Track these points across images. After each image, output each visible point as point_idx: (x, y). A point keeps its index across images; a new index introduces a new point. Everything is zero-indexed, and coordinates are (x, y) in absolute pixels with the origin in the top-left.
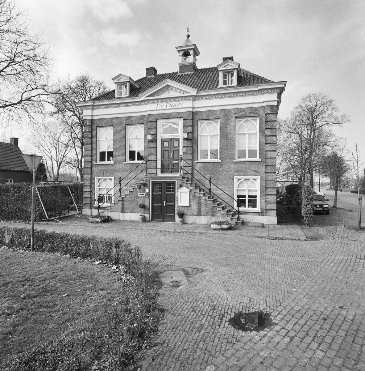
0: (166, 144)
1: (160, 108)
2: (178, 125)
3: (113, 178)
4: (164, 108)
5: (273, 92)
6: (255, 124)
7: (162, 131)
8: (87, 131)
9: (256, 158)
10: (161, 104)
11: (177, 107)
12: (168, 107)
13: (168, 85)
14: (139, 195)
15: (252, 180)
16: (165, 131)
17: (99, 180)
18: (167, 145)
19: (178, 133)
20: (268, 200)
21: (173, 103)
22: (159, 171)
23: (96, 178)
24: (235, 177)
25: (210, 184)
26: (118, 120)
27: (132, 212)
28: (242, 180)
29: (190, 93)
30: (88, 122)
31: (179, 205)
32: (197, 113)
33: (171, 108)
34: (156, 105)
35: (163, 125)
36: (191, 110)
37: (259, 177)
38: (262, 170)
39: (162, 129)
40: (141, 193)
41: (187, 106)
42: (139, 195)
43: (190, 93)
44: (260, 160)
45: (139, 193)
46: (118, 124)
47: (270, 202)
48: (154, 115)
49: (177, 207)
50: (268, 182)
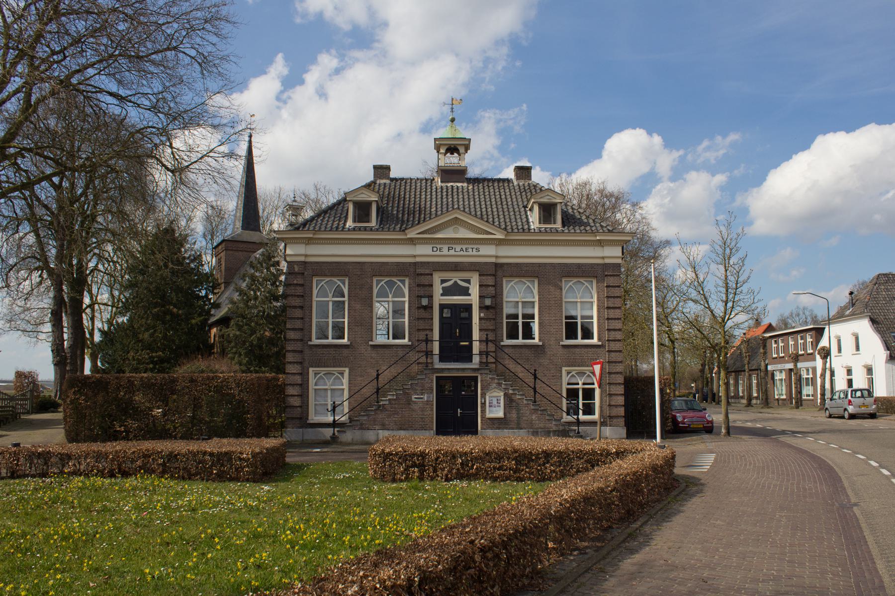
0: (447, 313)
2: (468, 281)
4: (445, 251)
5: (616, 245)
7: (441, 292)
8: (295, 282)
9: (593, 339)
11: (470, 253)
12: (452, 252)
15: (588, 373)
16: (446, 292)
18: (449, 315)
19: (469, 295)
20: (613, 403)
22: (436, 359)
23: (311, 369)
24: (564, 369)
25: (535, 380)
27: (401, 429)
28: (573, 373)
30: (296, 266)
32: (502, 265)
34: (430, 247)
35: (443, 281)
36: (493, 260)
39: (441, 287)
41: (488, 253)
46: (359, 273)
47: (616, 406)
50: (613, 376)
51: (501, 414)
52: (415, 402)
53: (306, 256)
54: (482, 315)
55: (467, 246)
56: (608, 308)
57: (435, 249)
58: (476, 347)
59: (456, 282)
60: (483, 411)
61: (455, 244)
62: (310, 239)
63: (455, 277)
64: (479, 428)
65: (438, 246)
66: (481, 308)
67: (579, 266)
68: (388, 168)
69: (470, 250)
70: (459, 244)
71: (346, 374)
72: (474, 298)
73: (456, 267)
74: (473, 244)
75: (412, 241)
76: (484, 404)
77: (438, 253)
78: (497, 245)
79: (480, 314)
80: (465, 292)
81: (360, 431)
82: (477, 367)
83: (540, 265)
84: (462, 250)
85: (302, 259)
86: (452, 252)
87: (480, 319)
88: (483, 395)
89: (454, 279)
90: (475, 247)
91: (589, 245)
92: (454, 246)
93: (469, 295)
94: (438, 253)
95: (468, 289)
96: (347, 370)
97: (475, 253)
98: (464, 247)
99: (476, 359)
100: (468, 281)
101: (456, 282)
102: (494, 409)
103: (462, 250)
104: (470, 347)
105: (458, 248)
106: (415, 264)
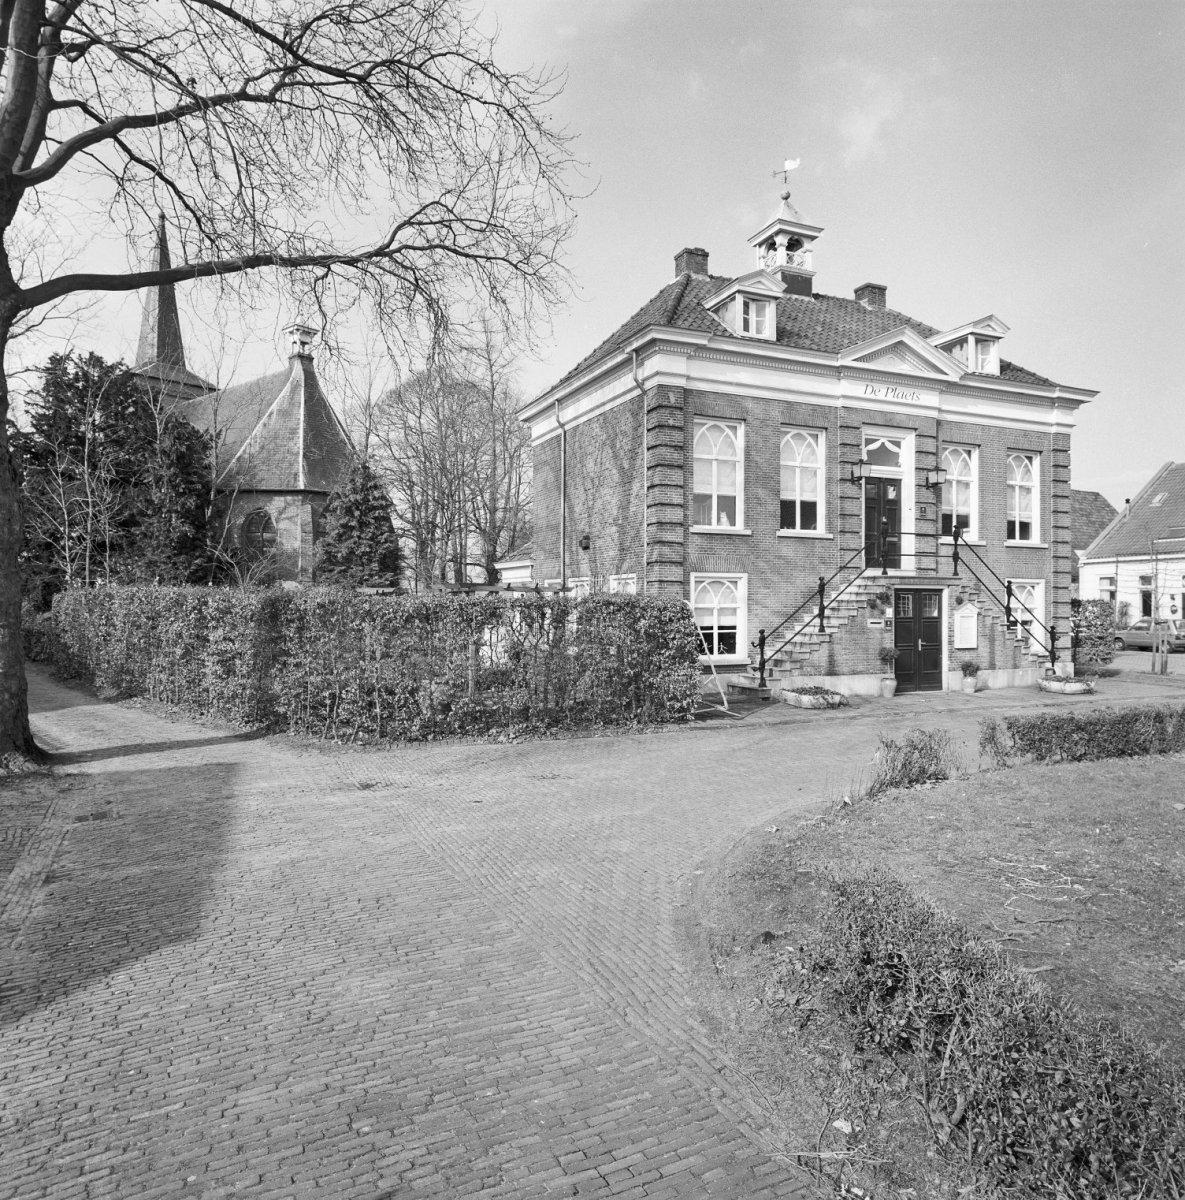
1: (872, 396)
2: (898, 444)
4: (881, 396)
6: (733, 437)
8: (671, 422)
10: (877, 386)
12: (890, 397)
13: (901, 343)
21: (900, 389)
26: (762, 405)
30: (671, 395)
31: (957, 645)
33: (896, 400)
35: (869, 442)
36: (934, 414)
38: (1050, 566)
44: (749, 532)
49: (951, 652)
56: (1056, 496)
58: (908, 544)
60: (951, 643)
62: (699, 347)
63: (883, 437)
71: (743, 585)
72: (906, 470)
73: (889, 423)
75: (839, 372)
78: (942, 392)
79: (899, 494)
88: (951, 616)
89: (883, 440)
93: (897, 464)
95: (897, 455)
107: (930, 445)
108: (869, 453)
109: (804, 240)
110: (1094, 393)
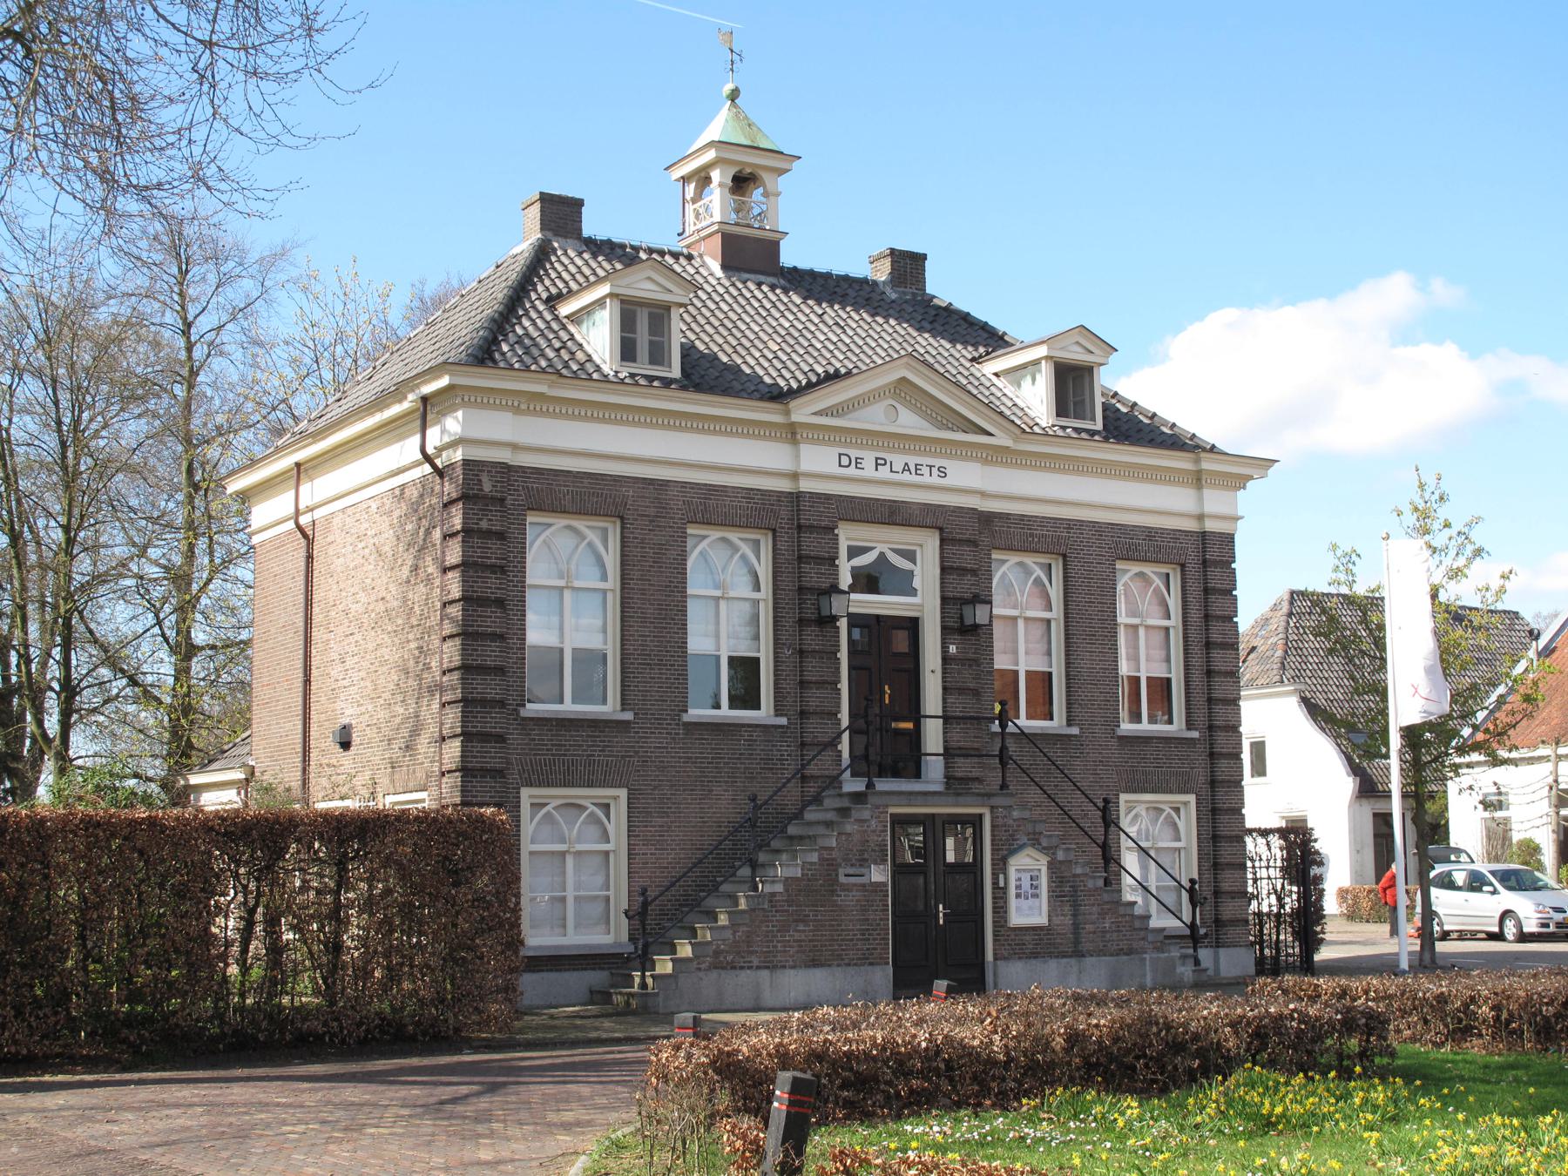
2: (910, 556)
3: (623, 793)
4: (869, 471)
8: (484, 525)
11: (926, 479)
12: (884, 473)
14: (842, 879)
17: (536, 806)
27: (814, 963)
29: (991, 435)
30: (485, 478)
34: (833, 452)
35: (854, 552)
37: (1192, 798)
40: (851, 871)
42: (842, 879)
43: (991, 435)
45: (841, 871)
46: (652, 512)
48: (828, 497)
51: (1042, 920)
52: (847, 888)
53: (515, 447)
54: (953, 649)
55: (919, 460)
57: (845, 461)
58: (933, 736)
59: (882, 555)
60: (1001, 909)
61: (892, 450)
63: (882, 542)
64: (989, 956)
65: (854, 453)
66: (945, 629)
67: (1151, 533)
68: (577, 204)
69: (925, 470)
70: (905, 451)
73: (891, 514)
74: (925, 453)
75: (792, 434)
76: (1001, 894)
77: (852, 471)
78: (986, 462)
80: (904, 583)
81: (714, 974)
82: (939, 788)
83: (1071, 524)
84: (906, 468)
85: (503, 456)
86: (884, 473)
87: (946, 659)
88: (1001, 865)
89: (881, 548)
90: (938, 462)
91: (1170, 482)
92: (888, 457)
93: (913, 593)
94: (852, 471)
96: (623, 793)
97: (935, 480)
98: (912, 461)
99: (934, 768)
100: (910, 556)
101: (882, 555)
102: (1024, 903)
103: (906, 468)
104: (916, 737)
105: (898, 461)
106: (797, 497)
107: (966, 557)
108: (856, 573)
109: (766, 176)
110: (1268, 463)
